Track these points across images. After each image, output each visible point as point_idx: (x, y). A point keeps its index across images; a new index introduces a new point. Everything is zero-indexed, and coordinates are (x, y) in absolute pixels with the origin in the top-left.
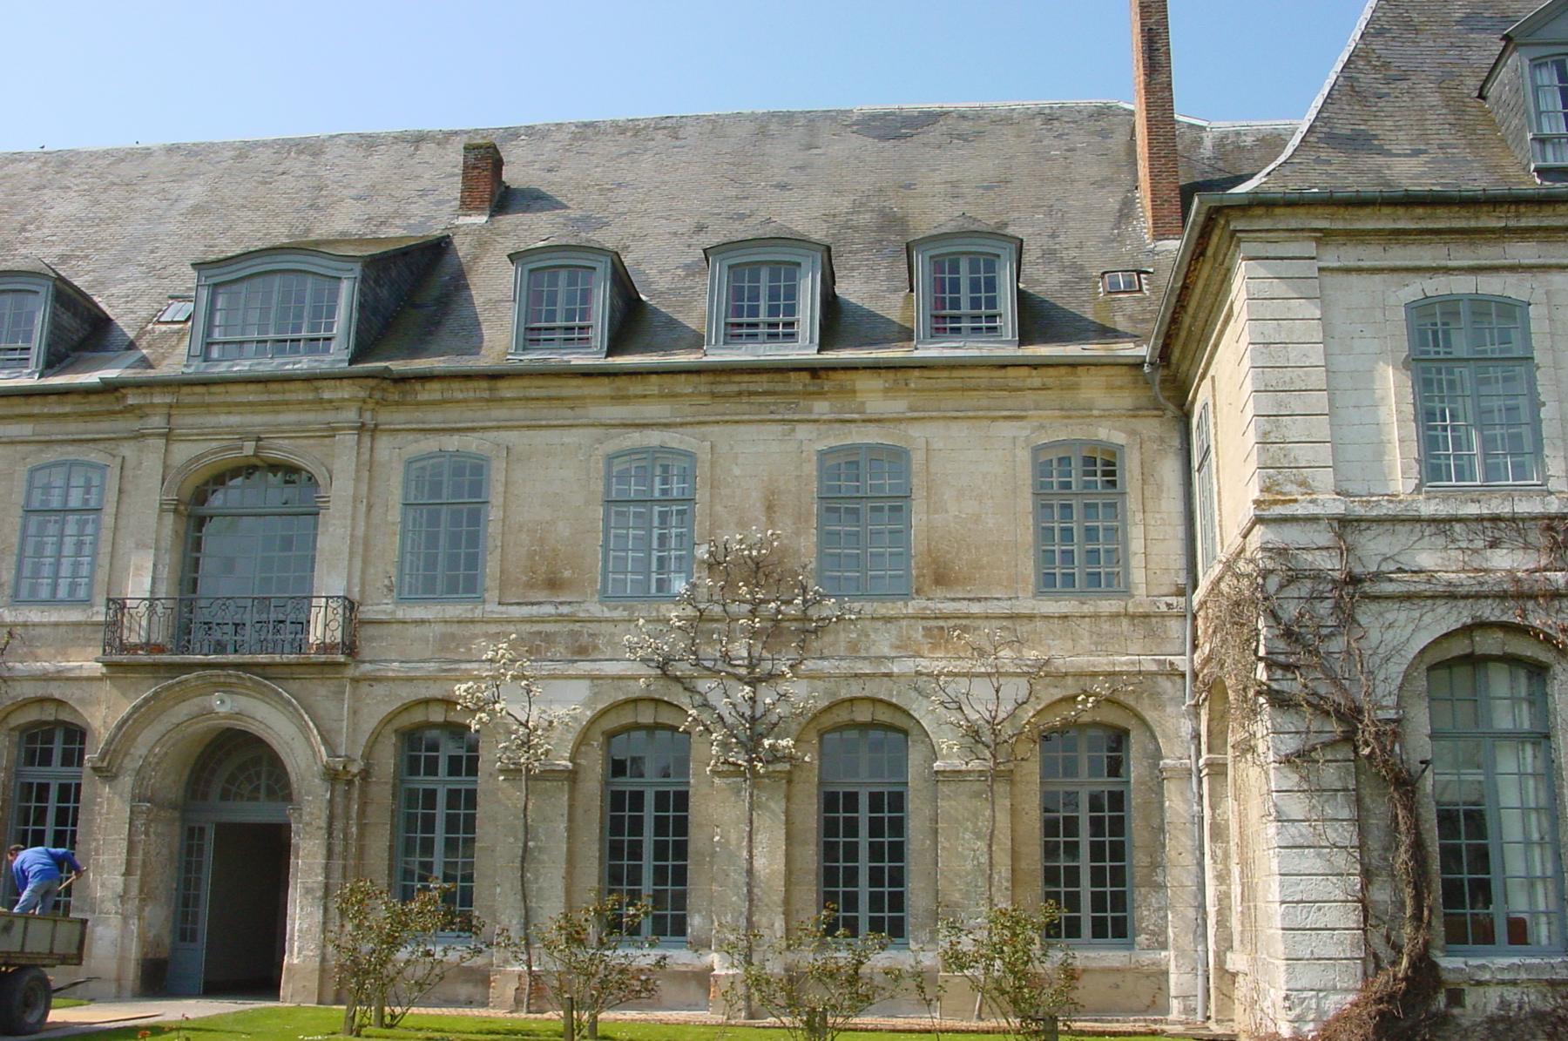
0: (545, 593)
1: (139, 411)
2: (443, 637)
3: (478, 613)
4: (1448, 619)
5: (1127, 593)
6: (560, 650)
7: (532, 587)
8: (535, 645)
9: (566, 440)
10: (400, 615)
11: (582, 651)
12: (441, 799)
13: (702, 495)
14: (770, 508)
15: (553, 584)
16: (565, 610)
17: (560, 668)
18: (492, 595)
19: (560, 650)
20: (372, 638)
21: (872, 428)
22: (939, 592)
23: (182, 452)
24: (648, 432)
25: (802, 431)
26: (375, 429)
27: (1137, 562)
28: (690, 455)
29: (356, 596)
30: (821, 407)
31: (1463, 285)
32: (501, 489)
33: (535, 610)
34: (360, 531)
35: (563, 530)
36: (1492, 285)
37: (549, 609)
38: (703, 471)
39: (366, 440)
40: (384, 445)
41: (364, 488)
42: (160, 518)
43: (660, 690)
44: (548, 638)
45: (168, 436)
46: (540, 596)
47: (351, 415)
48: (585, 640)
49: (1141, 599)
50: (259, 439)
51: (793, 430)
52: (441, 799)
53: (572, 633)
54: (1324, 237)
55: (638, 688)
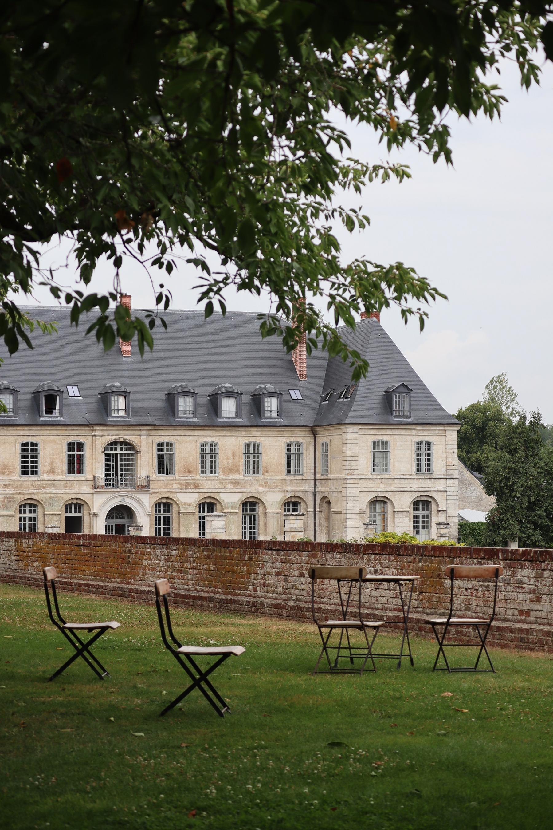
2: (167, 483)
3: (174, 479)
4: (375, 495)
5: (302, 475)
6: (192, 487)
8: (187, 485)
10: (158, 479)
11: (196, 487)
12: (162, 518)
14: (233, 456)
15: (189, 472)
16: (193, 478)
17: (193, 490)
19: (192, 487)
21: (254, 438)
22: (267, 474)
24: (208, 437)
25: (240, 438)
27: (305, 468)
33: (186, 478)
35: (191, 459)
37: (189, 478)
44: (189, 484)
46: (187, 474)
48: (196, 484)
49: (306, 476)
52: (162, 518)
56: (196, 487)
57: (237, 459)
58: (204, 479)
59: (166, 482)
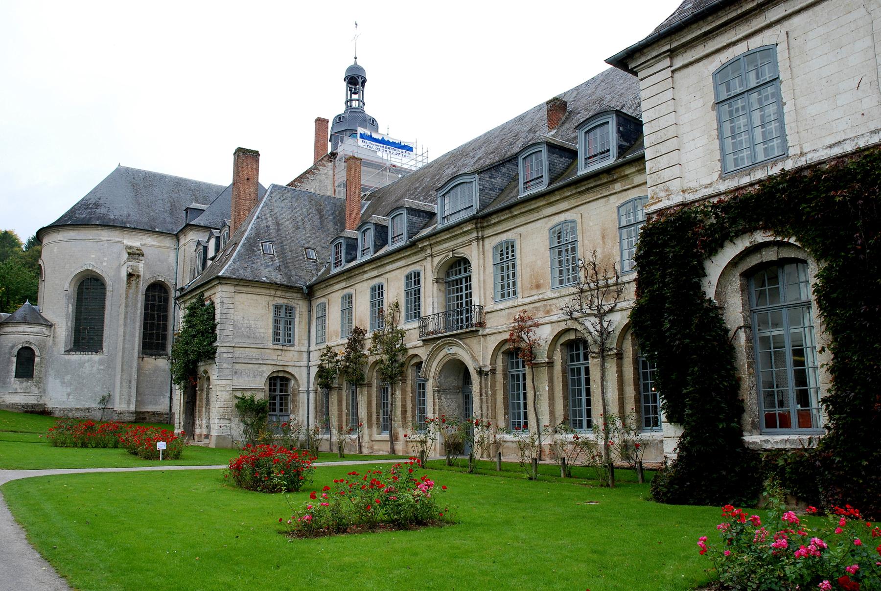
0: (536, 290)
1: (423, 249)
3: (516, 304)
7: (532, 289)
9: (537, 226)
13: (579, 238)
14: (603, 237)
15: (538, 287)
16: (541, 296)
18: (519, 295)
20: (490, 318)
21: (636, 189)
23: (437, 260)
26: (483, 238)
28: (574, 221)
29: (482, 304)
30: (618, 187)
31: (740, 50)
32: (519, 251)
34: (482, 279)
36: (755, 43)
37: (535, 298)
38: (579, 227)
39: (481, 243)
40: (487, 241)
41: (481, 261)
42: (433, 285)
43: (572, 324)
45: (431, 256)
46: (534, 292)
47: (474, 235)
48: (548, 307)
50: (453, 251)
51: (609, 200)
53: (545, 306)
54: (672, 53)
55: (563, 326)
56: (548, 312)
57: (609, 242)
58: (557, 295)
59: (507, 311)
